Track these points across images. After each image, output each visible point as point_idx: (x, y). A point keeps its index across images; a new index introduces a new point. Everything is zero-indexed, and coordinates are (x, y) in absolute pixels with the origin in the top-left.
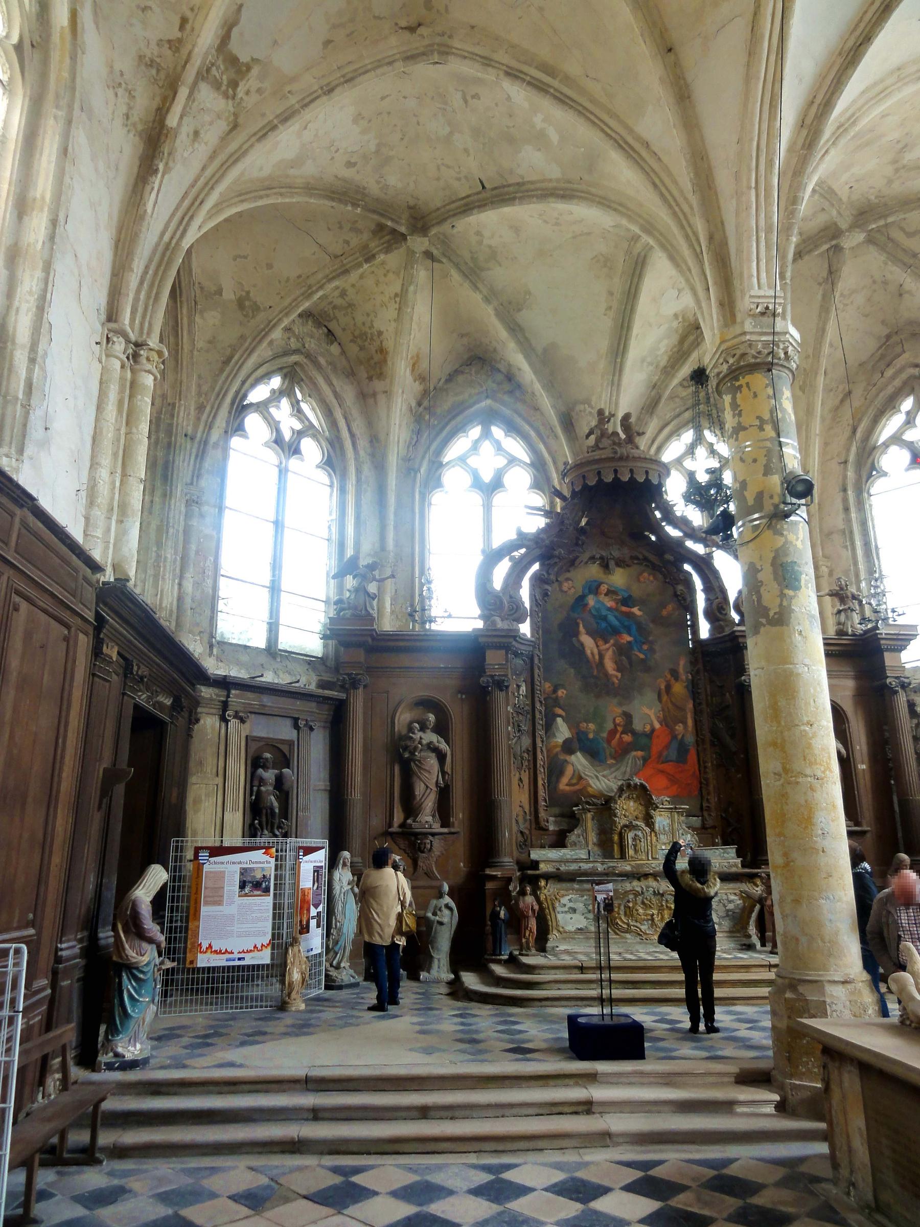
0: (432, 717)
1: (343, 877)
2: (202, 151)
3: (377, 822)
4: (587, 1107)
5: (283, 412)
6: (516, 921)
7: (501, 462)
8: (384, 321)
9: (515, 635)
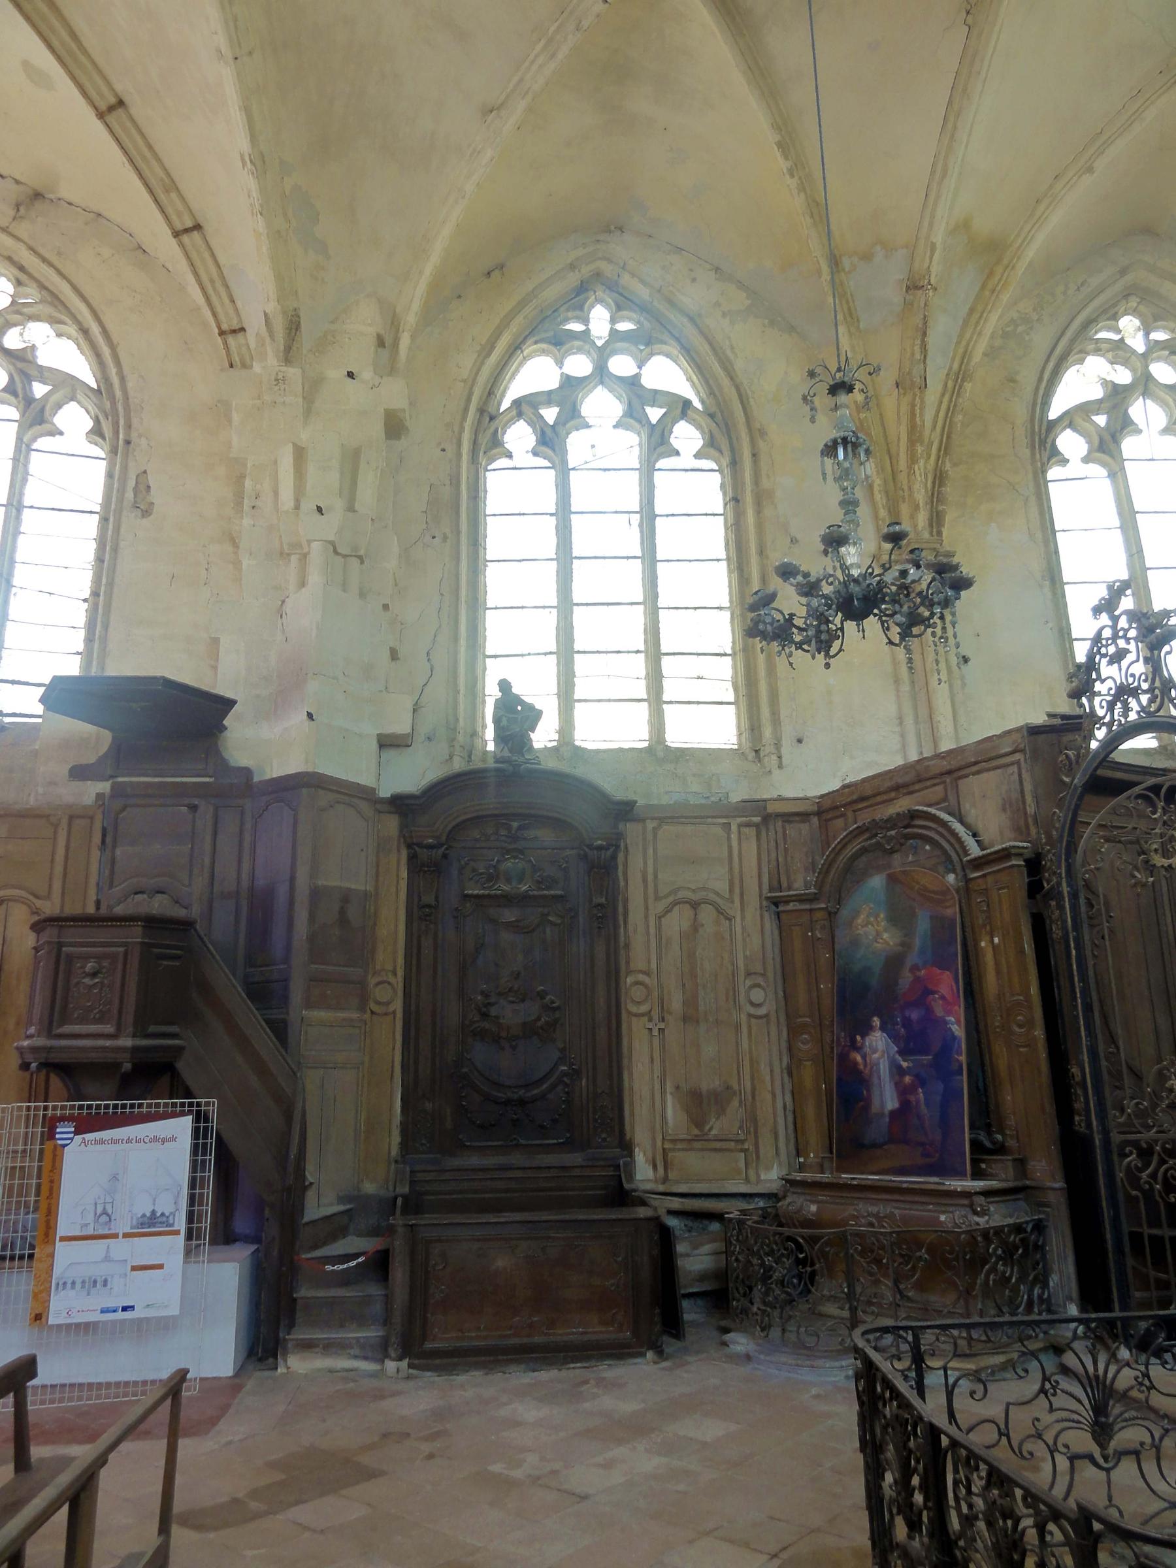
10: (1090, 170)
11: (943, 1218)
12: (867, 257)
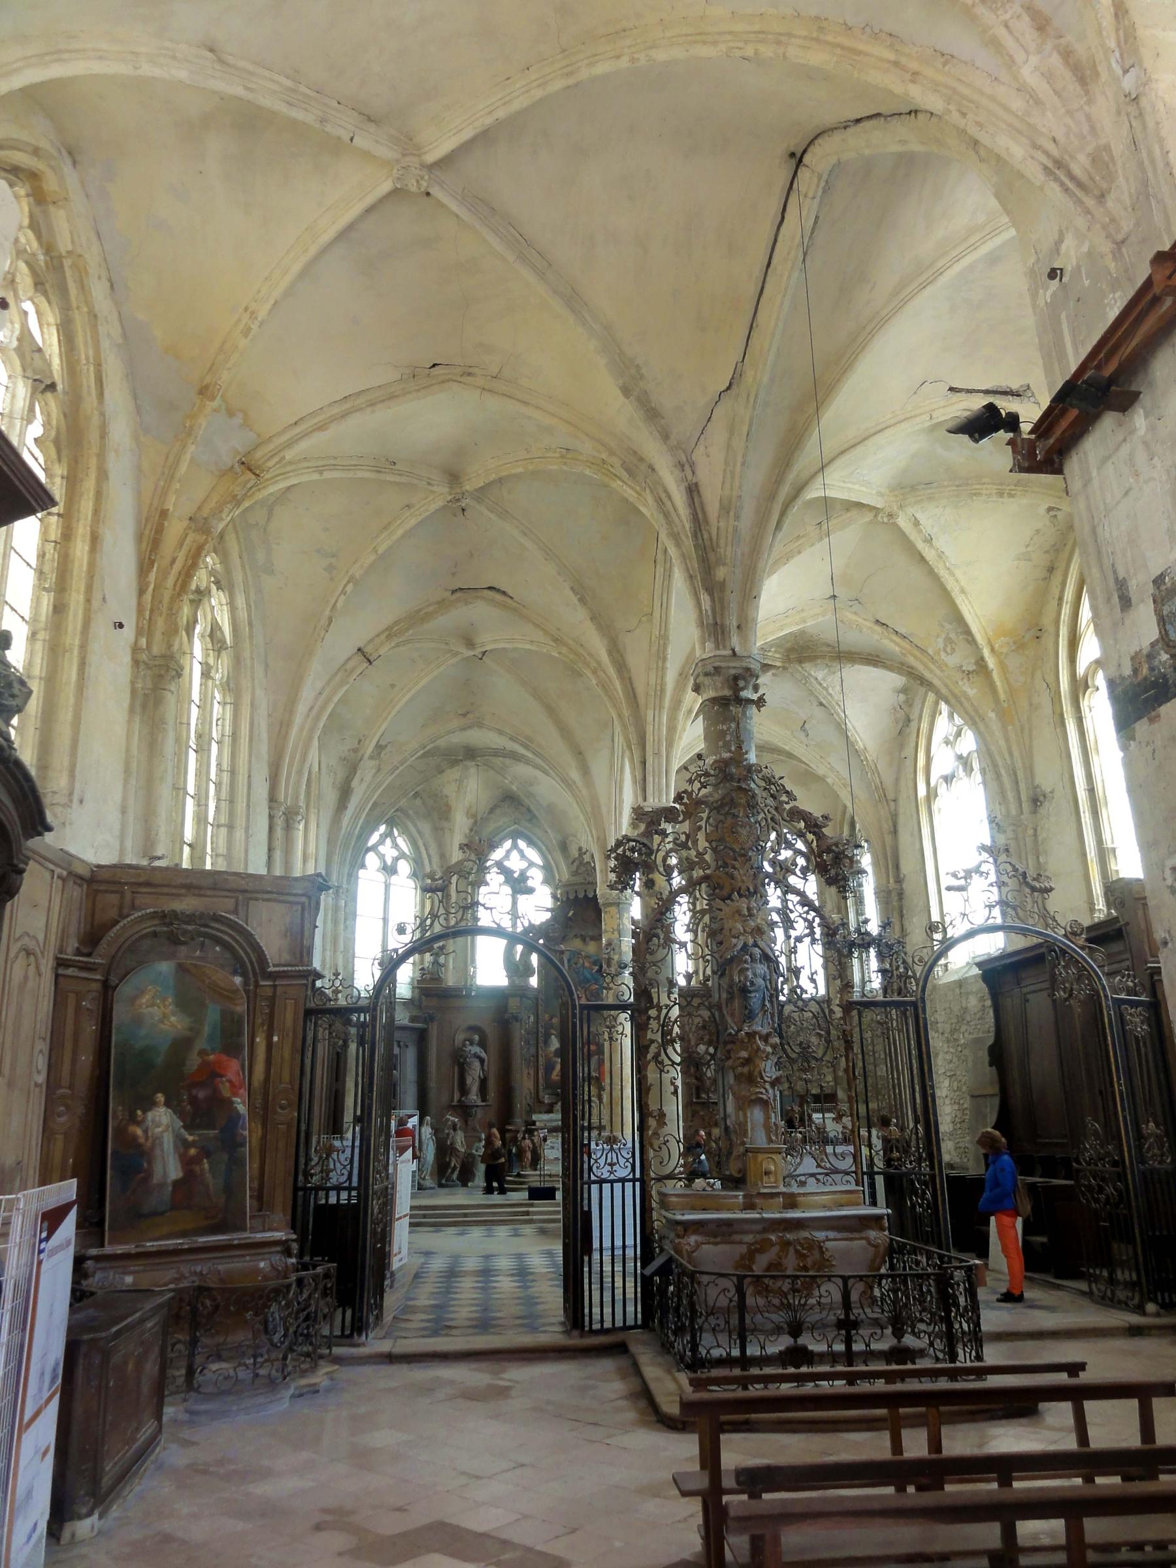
0: (477, 1037)
1: (427, 1131)
2: (364, 786)
3: (445, 1099)
4: (527, 1213)
5: (388, 851)
6: (521, 1153)
7: (524, 865)
8: (450, 790)
9: (529, 987)
10: (321, 472)
11: (262, 1265)
12: (231, 413)
